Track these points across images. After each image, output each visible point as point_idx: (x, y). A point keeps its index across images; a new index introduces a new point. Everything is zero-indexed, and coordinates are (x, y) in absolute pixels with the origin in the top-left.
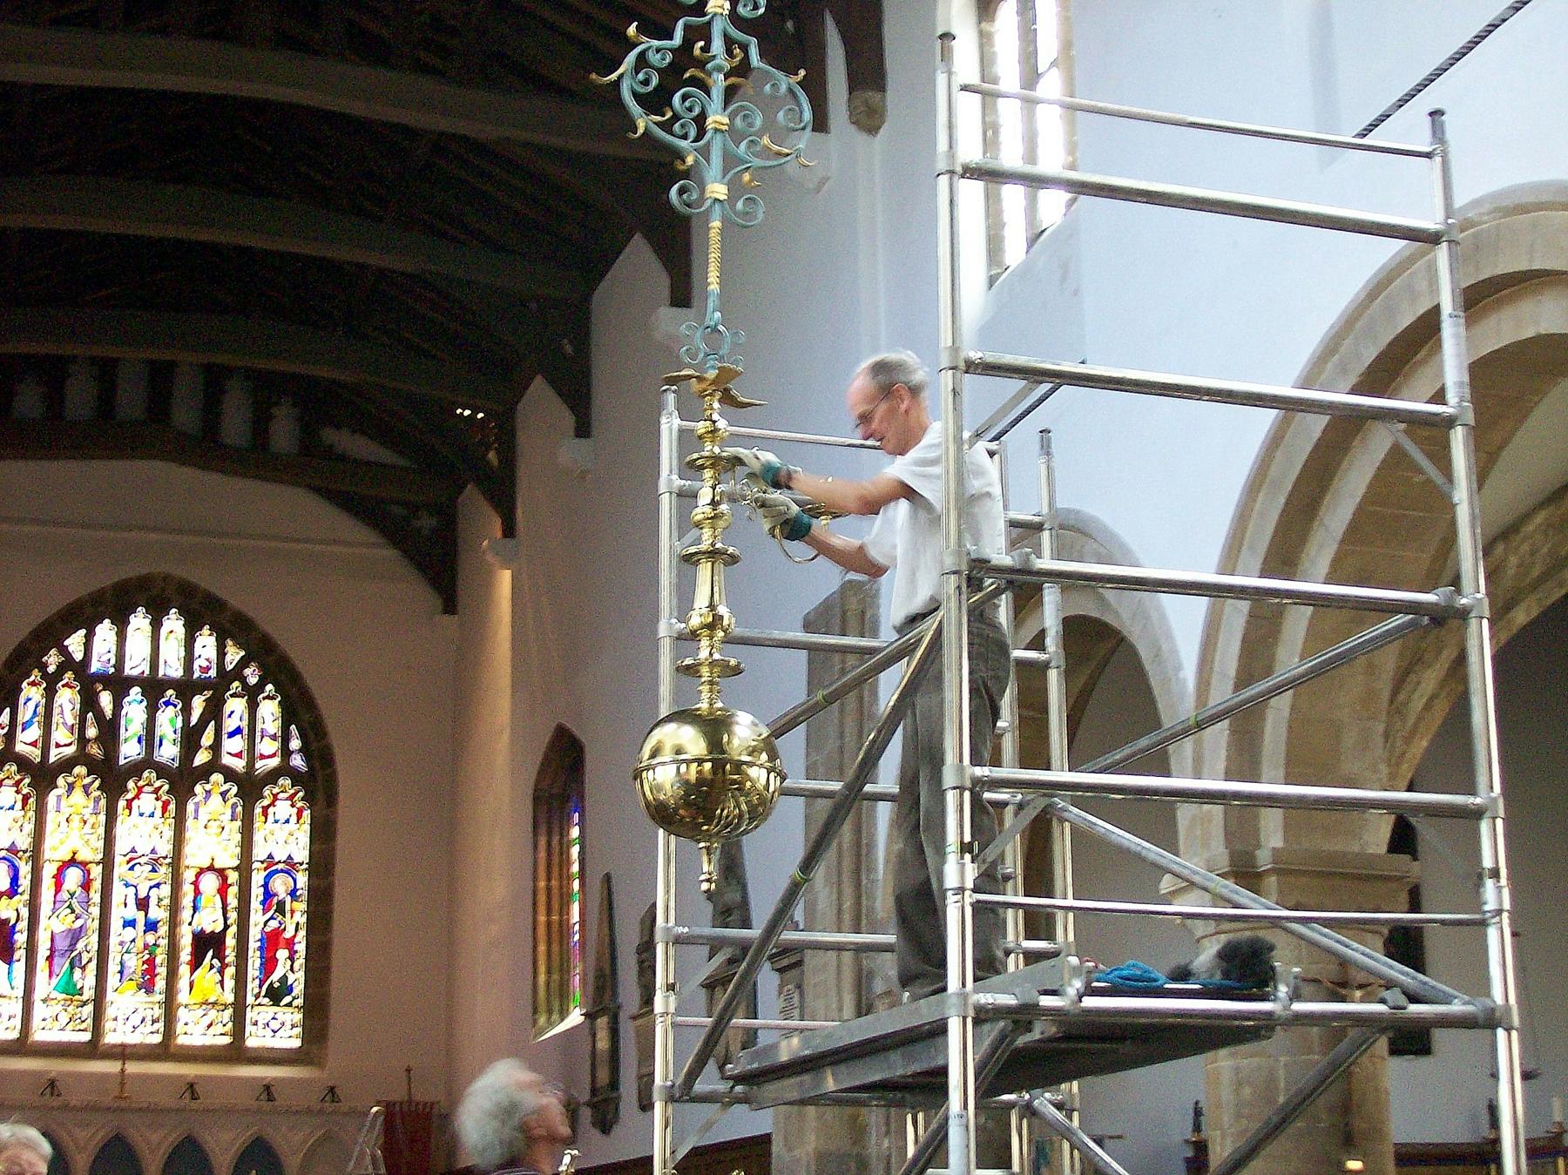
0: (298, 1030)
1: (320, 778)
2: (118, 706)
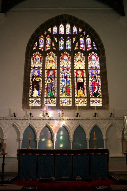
0: (101, 103)
1: (100, 51)
2: (59, 40)
